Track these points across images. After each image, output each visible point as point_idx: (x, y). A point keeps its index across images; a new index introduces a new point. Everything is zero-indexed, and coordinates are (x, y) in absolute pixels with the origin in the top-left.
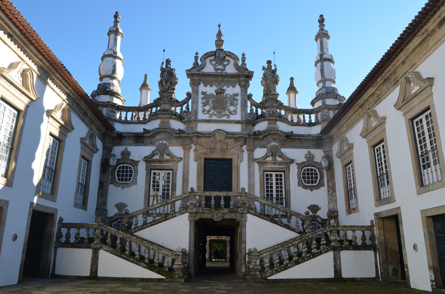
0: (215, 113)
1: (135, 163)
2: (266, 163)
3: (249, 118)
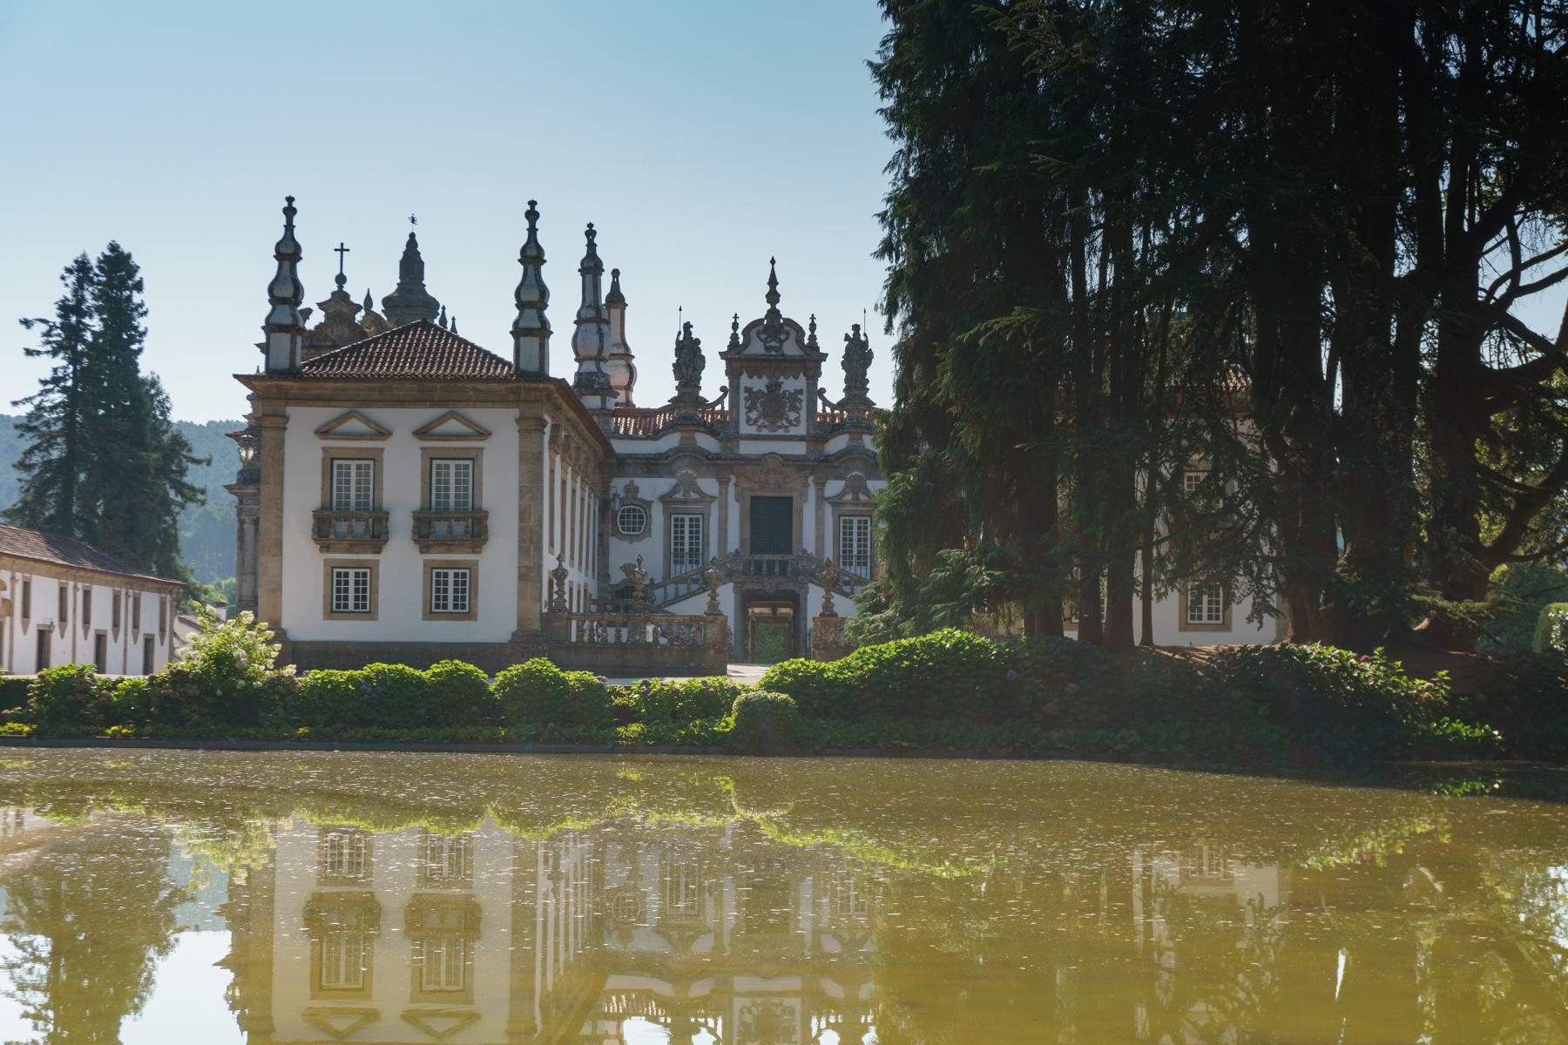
0: (766, 423)
1: (648, 504)
2: (843, 504)
3: (819, 432)
